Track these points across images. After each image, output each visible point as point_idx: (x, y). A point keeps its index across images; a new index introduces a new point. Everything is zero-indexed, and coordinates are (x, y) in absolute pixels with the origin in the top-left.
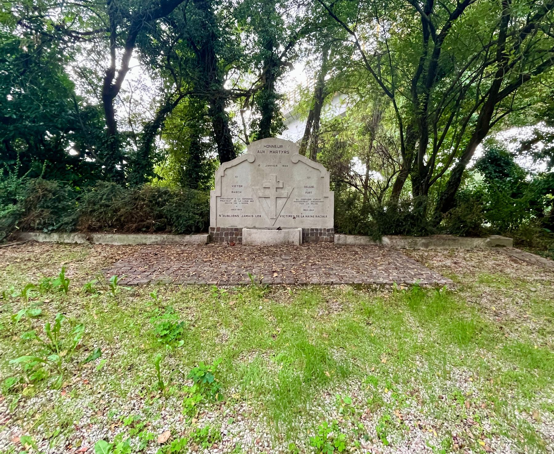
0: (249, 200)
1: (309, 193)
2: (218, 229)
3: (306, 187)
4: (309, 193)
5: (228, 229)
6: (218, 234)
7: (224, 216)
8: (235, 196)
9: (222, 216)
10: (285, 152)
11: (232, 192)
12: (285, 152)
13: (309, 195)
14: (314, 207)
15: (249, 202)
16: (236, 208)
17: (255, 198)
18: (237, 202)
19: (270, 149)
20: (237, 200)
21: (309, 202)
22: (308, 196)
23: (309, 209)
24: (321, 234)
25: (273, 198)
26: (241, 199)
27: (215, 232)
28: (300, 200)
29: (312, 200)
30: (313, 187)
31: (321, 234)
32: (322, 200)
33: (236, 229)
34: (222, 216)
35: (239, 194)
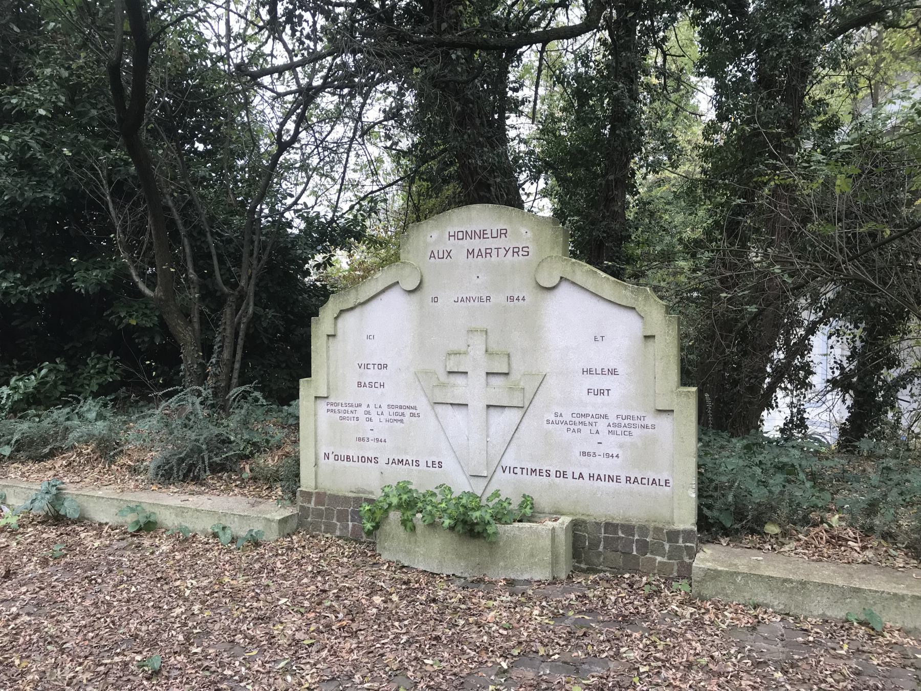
0: (407, 412)
1: (601, 392)
2: (321, 497)
3: (589, 371)
4: (601, 392)
5: (346, 499)
6: (319, 514)
7: (337, 458)
8: (368, 397)
9: (332, 457)
11: (359, 384)
14: (621, 446)
16: (371, 435)
17: (423, 405)
18: (373, 415)
19: (468, 244)
20: (372, 406)
21: (602, 425)
22: (595, 404)
23: (602, 450)
25: (477, 404)
27: (312, 505)
28: (567, 417)
29: (612, 419)
30: (613, 372)
31: (644, 547)
32: (649, 421)
34: (332, 457)
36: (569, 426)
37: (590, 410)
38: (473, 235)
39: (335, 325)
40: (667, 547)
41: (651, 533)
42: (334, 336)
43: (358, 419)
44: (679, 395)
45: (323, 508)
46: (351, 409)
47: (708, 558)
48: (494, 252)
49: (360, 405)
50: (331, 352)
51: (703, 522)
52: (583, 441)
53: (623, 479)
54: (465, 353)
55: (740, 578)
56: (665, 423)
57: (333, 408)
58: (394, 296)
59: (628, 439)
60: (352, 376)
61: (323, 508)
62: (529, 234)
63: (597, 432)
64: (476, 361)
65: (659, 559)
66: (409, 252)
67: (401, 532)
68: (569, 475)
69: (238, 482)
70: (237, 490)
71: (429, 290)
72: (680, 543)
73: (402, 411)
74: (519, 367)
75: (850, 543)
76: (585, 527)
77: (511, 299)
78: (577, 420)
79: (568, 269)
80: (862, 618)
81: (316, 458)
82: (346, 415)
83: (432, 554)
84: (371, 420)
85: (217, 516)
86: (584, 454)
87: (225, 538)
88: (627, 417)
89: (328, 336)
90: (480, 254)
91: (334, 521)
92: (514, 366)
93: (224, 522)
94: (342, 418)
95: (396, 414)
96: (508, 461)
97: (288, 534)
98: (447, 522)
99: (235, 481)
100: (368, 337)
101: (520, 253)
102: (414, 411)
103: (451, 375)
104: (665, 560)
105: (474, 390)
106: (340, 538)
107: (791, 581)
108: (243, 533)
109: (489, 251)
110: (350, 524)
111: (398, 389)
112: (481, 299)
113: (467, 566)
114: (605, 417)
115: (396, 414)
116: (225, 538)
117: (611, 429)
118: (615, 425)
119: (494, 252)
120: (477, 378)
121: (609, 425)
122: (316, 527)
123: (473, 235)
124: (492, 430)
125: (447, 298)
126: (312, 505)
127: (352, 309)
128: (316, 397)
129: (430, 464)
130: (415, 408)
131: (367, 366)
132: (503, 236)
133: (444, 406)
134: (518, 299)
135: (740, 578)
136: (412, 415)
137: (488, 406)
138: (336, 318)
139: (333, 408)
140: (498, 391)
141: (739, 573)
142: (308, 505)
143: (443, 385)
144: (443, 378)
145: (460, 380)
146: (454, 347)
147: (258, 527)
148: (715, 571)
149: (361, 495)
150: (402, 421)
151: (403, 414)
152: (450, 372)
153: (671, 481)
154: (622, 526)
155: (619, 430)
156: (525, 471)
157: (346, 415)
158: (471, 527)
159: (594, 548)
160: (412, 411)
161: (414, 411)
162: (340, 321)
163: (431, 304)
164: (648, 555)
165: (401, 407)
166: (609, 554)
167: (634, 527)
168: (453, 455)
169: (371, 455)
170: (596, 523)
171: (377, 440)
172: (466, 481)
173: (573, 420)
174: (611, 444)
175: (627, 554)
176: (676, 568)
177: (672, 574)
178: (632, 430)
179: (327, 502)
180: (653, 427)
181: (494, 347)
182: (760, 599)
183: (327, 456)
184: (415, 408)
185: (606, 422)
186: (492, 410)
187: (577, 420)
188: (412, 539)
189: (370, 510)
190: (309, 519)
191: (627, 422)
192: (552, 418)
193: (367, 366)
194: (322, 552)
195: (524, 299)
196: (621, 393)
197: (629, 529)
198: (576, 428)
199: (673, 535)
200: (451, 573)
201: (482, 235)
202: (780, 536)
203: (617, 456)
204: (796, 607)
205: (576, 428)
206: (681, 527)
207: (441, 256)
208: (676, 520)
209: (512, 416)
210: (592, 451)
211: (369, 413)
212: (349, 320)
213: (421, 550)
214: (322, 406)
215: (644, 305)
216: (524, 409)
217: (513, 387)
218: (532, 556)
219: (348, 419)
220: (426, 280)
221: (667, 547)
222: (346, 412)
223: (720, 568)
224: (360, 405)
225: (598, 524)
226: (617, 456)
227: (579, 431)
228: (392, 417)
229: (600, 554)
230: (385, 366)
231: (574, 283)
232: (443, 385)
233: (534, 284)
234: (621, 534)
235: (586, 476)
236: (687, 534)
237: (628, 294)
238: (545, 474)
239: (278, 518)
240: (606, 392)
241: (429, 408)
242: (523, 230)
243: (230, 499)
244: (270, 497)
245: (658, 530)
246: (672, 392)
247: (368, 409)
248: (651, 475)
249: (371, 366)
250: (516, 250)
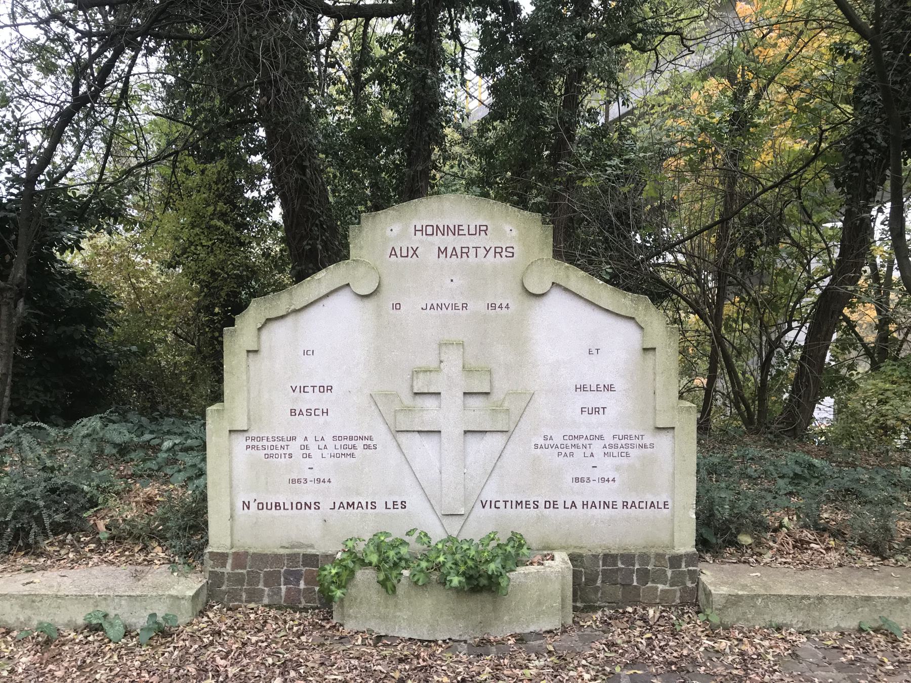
0: (360, 444)
1: (596, 410)
2: (240, 558)
3: (583, 388)
4: (596, 410)
5: (277, 558)
6: (239, 579)
7: (261, 506)
8: (306, 427)
9: (253, 506)
11: (293, 412)
14: (617, 468)
16: (309, 475)
17: (381, 435)
18: (313, 450)
19: (439, 241)
20: (311, 440)
21: (597, 446)
22: (588, 425)
23: (597, 474)
24: (644, 575)
27: (228, 568)
28: (558, 440)
29: (608, 440)
30: (609, 388)
31: (644, 575)
32: (647, 440)
34: (253, 506)
35: (322, 419)
36: (560, 450)
37: (585, 432)
38: (446, 230)
39: (259, 337)
40: (669, 573)
41: (653, 560)
42: (256, 351)
43: (291, 456)
44: (681, 410)
45: (244, 571)
46: (281, 443)
47: (717, 579)
48: (472, 252)
49: (293, 438)
50: (252, 373)
51: (702, 543)
52: (578, 465)
53: (620, 505)
54: (438, 370)
55: (760, 600)
56: (664, 442)
57: (255, 443)
58: (343, 300)
59: (625, 461)
60: (283, 403)
61: (244, 571)
62: (515, 233)
63: (592, 455)
64: (451, 378)
65: (661, 587)
66: (361, 248)
67: (374, 594)
68: (560, 504)
69: (92, 546)
70: (96, 558)
71: (388, 297)
72: (683, 568)
73: (353, 442)
74: (501, 387)
75: (812, 545)
76: (582, 562)
77: (493, 306)
78: (569, 443)
79: (562, 273)
80: (876, 625)
81: (232, 509)
82: (274, 452)
83: (420, 617)
84: (309, 456)
85: (91, 601)
86: (577, 480)
87: (115, 631)
88: (624, 437)
89: (248, 351)
91: (261, 586)
92: (496, 384)
93: (103, 608)
94: (268, 456)
95: (345, 447)
96: (489, 494)
97: (201, 612)
98: (456, 580)
99: (87, 544)
100: (306, 353)
101: (504, 254)
102: (369, 442)
103: (417, 397)
104: (667, 587)
105: (448, 414)
106: (270, 606)
107: (808, 598)
108: (140, 620)
109: (465, 250)
110: (283, 588)
111: (348, 416)
112: (455, 307)
113: (467, 627)
114: (601, 437)
115: (345, 447)
116: (115, 631)
117: (606, 451)
118: (611, 446)
119: (472, 252)
120: (453, 399)
121: (605, 447)
122: (234, 595)
123: (446, 230)
124: (470, 459)
125: (412, 304)
126: (228, 568)
127: (282, 317)
128: (230, 431)
129: (390, 505)
130: (371, 438)
131: (303, 389)
132: (483, 233)
133: (409, 435)
134: (501, 307)
135: (760, 600)
136: (367, 447)
137: (466, 432)
138: (259, 329)
139: (255, 443)
140: (478, 413)
141: (759, 596)
142: (222, 570)
143: (408, 410)
144: (408, 400)
145: (430, 402)
146: (421, 363)
147: (161, 611)
148: (737, 596)
149: (296, 550)
150: (352, 455)
151: (354, 447)
152: (416, 394)
153: (670, 503)
154: (622, 555)
155: (615, 452)
156: (509, 504)
157: (274, 452)
158: (479, 581)
159: (604, 583)
160: (366, 442)
161: (369, 442)
162: (265, 332)
163: (391, 312)
164: (650, 584)
165: (351, 438)
166: (608, 588)
167: (634, 556)
168: (421, 492)
169: (309, 499)
170: (593, 555)
171: (319, 480)
172: (438, 523)
173: (565, 442)
174: (607, 466)
175: (627, 585)
176: (678, 594)
177: (674, 601)
178: (629, 450)
179: (249, 563)
180: (652, 446)
181: (472, 363)
182: (779, 620)
184: (371, 438)
185: (602, 443)
186: (469, 436)
187: (569, 443)
188: (391, 602)
189: (337, 573)
190: (224, 588)
191: (624, 442)
192: (541, 441)
193: (303, 389)
194: (259, 631)
195: (507, 307)
196: (617, 413)
197: (628, 558)
198: (568, 451)
199: (675, 561)
200: (446, 638)
201: (457, 231)
202: (753, 545)
203: (614, 480)
204: (814, 623)
205: (568, 451)
206: (682, 550)
207: (404, 254)
208: (676, 543)
209: (494, 442)
210: (586, 476)
211: (306, 447)
212: (279, 332)
213: (404, 614)
214: (240, 442)
215: (645, 315)
216: (509, 434)
217: (494, 407)
218: (539, 603)
219: (277, 456)
220: (385, 281)
221: (669, 573)
222: (273, 447)
223: (740, 593)
224: (293, 438)
225: (595, 557)
226: (614, 480)
227: (572, 454)
228: (339, 451)
229: (597, 589)
231: (566, 290)
232: (408, 410)
233: (520, 289)
234: (620, 565)
235: (579, 504)
236: (691, 559)
237: (628, 302)
238: (532, 505)
239: (191, 593)
240: (601, 410)
241: (389, 437)
242: (507, 228)
243: (95, 571)
244: (150, 562)
245: (660, 556)
246: (673, 407)
247: (306, 443)
248: (650, 498)
249: (310, 389)
250: (498, 250)
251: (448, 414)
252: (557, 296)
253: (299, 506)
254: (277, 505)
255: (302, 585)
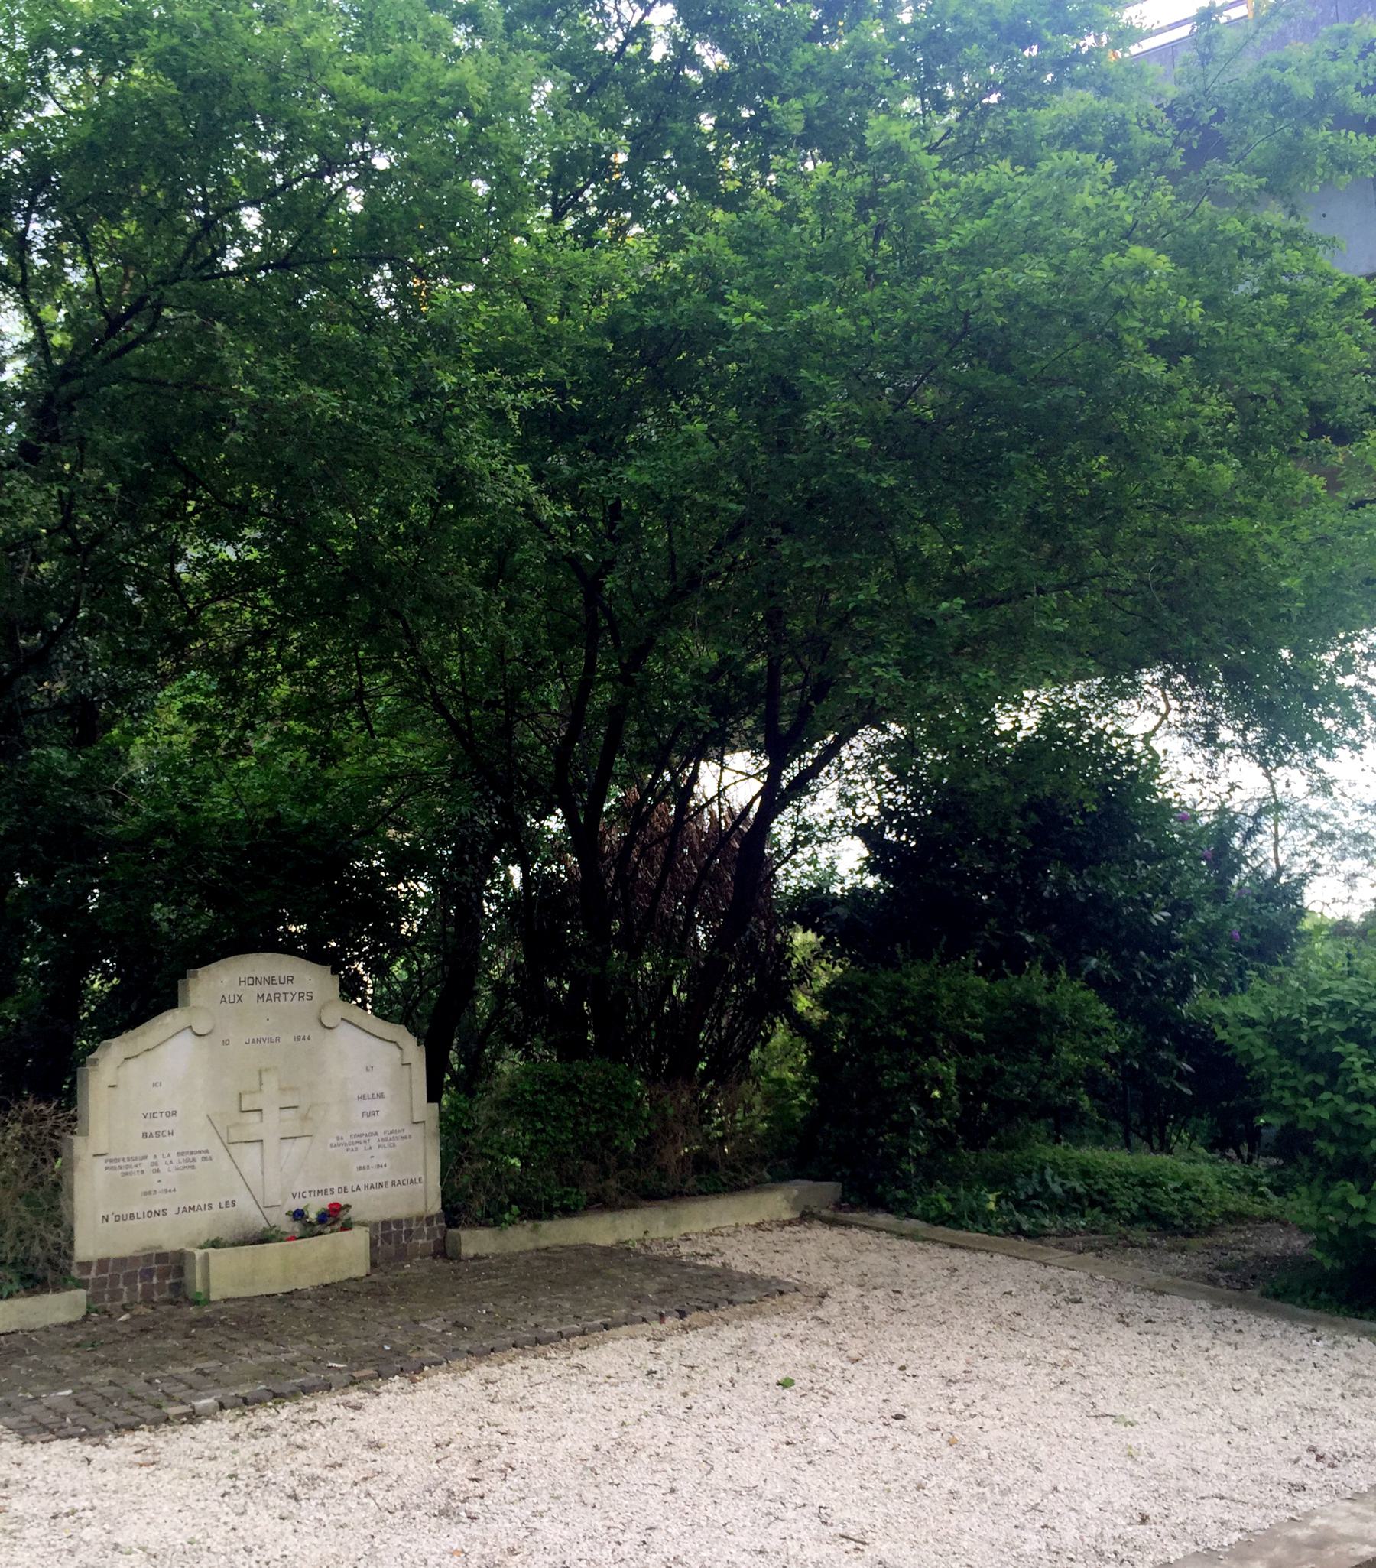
0: (199, 1157)
1: (372, 1114)
2: (103, 1264)
3: (363, 1097)
4: (372, 1114)
5: (134, 1259)
9: (111, 1219)
10: (301, 996)
11: (145, 1135)
12: (301, 996)
13: (372, 1119)
14: (388, 1156)
15: (199, 1163)
18: (162, 1167)
19: (257, 989)
22: (367, 1125)
23: (375, 1161)
26: (174, 1157)
27: (93, 1274)
28: (347, 1139)
29: (381, 1135)
30: (381, 1096)
31: (409, 1232)
32: (406, 1133)
33: (162, 1257)
34: (111, 1219)
35: (168, 1139)
37: (365, 1131)
77: (298, 1038)
90: (269, 999)
105: (271, 1125)
120: (272, 1115)
131: (153, 1116)
140: (290, 1122)
145: (255, 1116)
169: (158, 1208)
183: (106, 1219)
192: (334, 1141)
193: (153, 1116)
197: (398, 1223)
201: (271, 981)
230: (175, 1113)
245: (419, 1219)
248: (409, 1176)
251: (271, 1125)
252: (345, 1028)
253: (149, 1214)
254: (132, 1216)
255: (155, 1280)
